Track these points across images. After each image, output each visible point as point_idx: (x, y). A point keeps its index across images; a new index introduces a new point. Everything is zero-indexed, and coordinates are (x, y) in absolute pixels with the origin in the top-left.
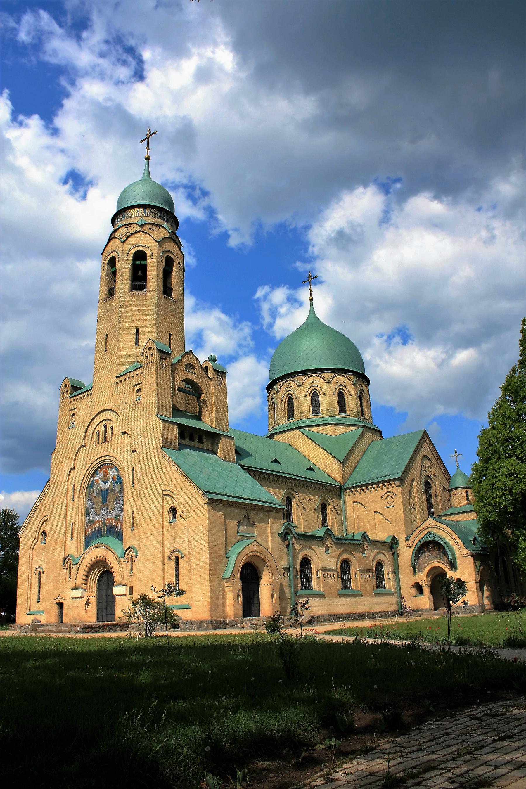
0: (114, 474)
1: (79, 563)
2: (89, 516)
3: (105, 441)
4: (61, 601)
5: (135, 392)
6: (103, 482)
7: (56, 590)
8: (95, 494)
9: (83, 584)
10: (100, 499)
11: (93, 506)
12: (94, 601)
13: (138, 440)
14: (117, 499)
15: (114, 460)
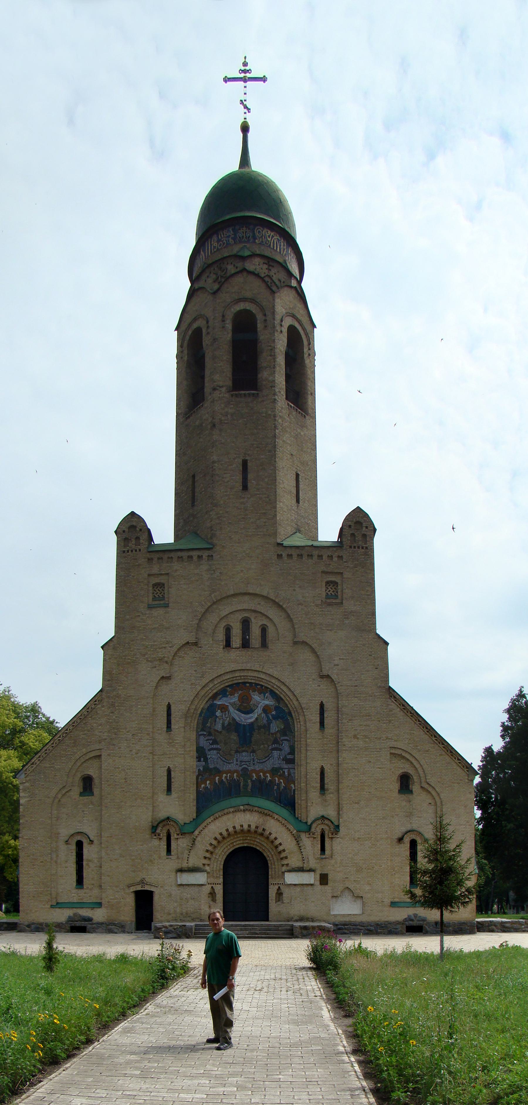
0: (267, 702)
1: (196, 832)
2: (206, 760)
3: (246, 644)
4: (147, 888)
5: (324, 584)
6: (239, 710)
7: (134, 871)
8: (219, 727)
9: (204, 865)
10: (234, 737)
11: (215, 746)
12: (219, 890)
13: (336, 662)
14: (276, 742)
15: (273, 681)
